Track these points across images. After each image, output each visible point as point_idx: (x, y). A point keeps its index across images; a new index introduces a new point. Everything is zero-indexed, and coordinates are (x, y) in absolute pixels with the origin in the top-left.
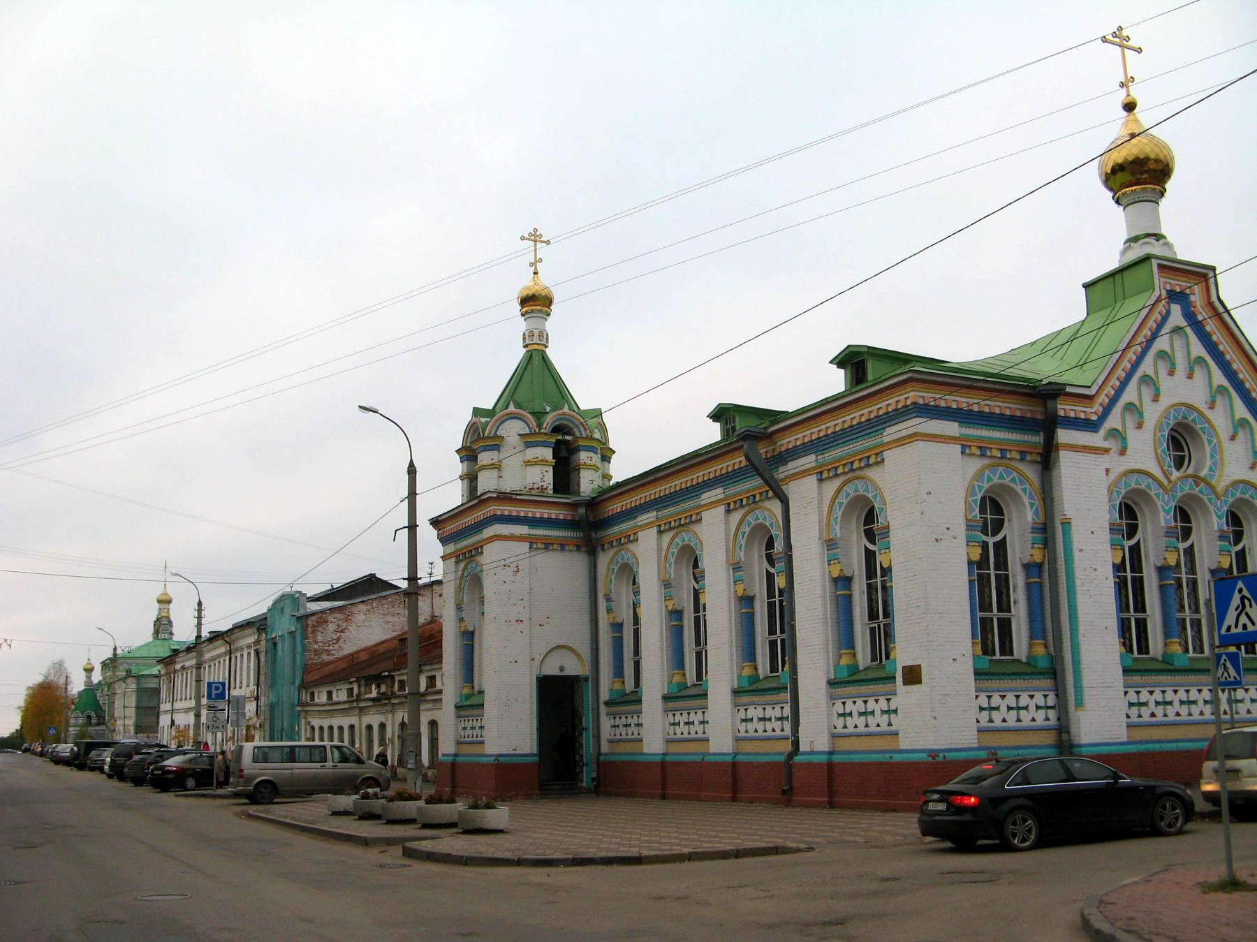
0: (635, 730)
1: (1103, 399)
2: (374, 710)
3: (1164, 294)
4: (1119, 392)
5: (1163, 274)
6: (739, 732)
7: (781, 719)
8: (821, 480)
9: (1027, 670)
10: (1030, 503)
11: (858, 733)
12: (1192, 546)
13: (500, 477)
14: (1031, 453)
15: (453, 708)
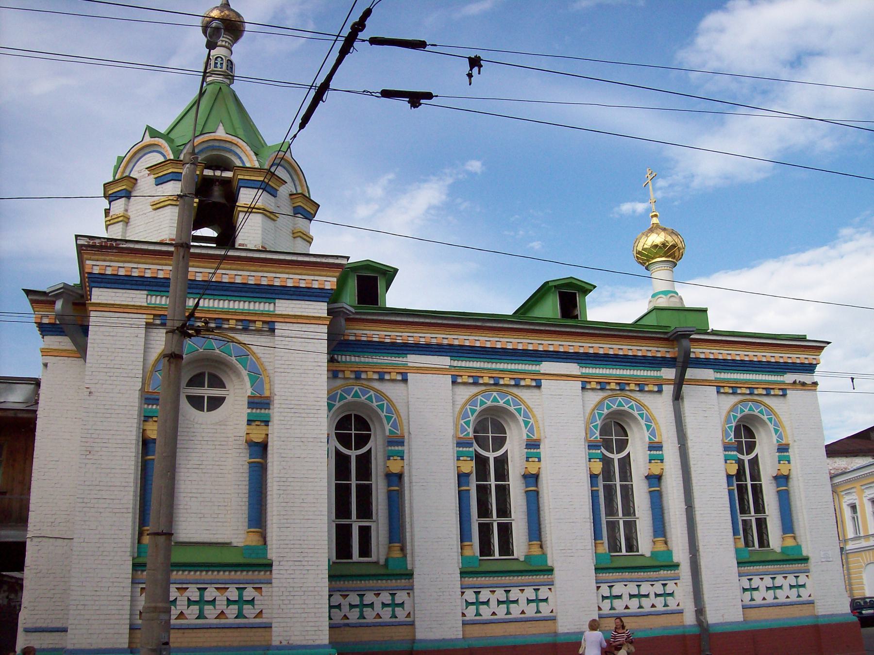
11: (778, 603)
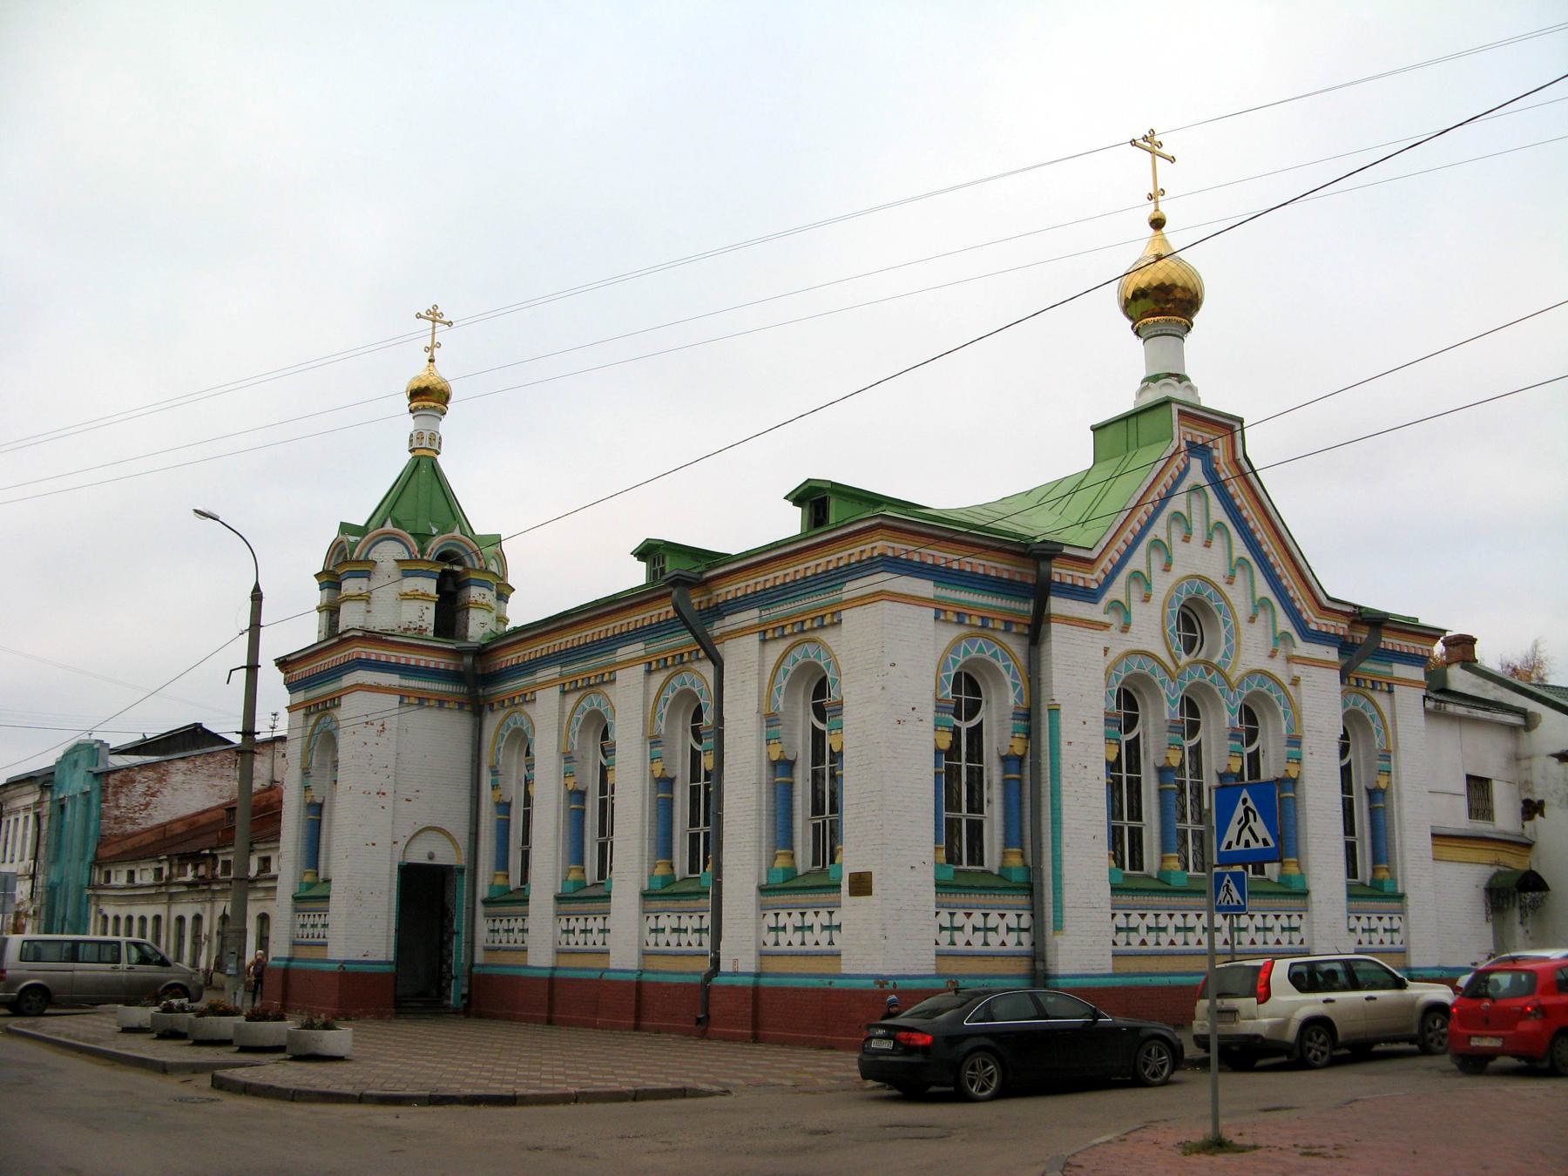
0: (519, 936)
1: (1105, 564)
2: (190, 897)
3: (1183, 444)
4: (1125, 557)
5: (1184, 422)
6: (647, 945)
7: (699, 931)
8: (764, 641)
9: (999, 884)
10: (1012, 682)
11: (792, 952)
12: (1199, 744)
13: (369, 612)
14: (1017, 623)
15: (290, 900)
